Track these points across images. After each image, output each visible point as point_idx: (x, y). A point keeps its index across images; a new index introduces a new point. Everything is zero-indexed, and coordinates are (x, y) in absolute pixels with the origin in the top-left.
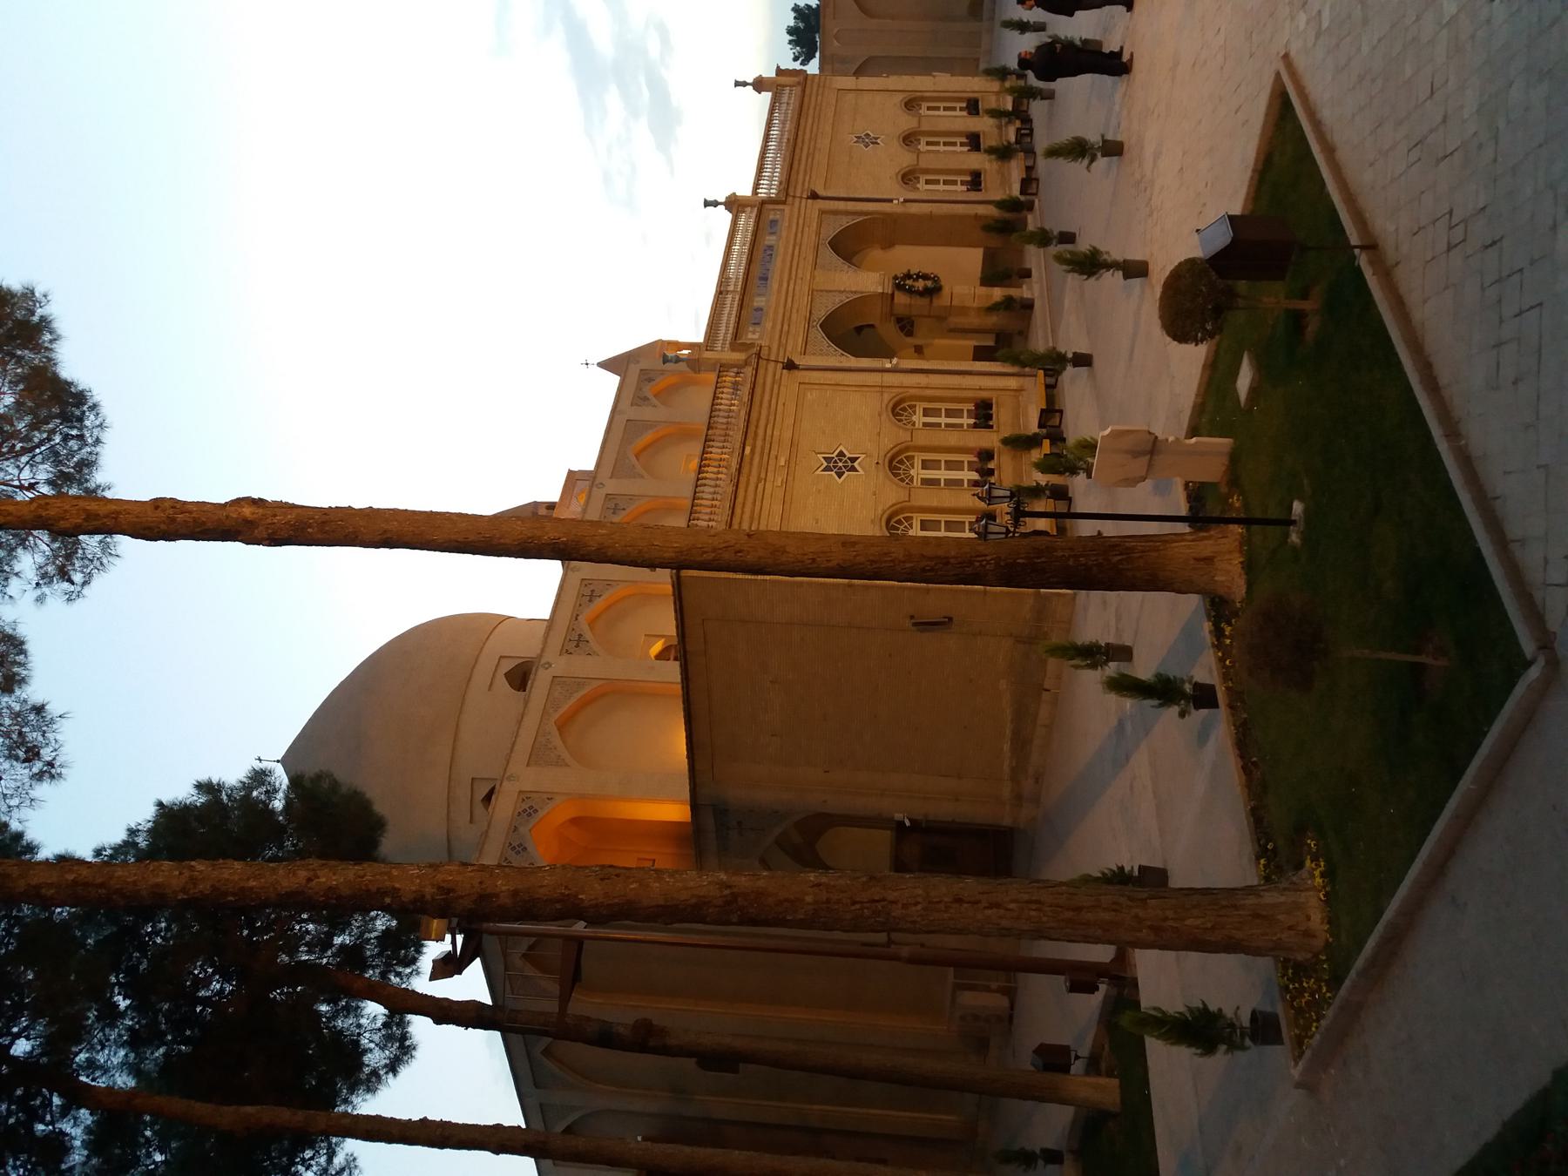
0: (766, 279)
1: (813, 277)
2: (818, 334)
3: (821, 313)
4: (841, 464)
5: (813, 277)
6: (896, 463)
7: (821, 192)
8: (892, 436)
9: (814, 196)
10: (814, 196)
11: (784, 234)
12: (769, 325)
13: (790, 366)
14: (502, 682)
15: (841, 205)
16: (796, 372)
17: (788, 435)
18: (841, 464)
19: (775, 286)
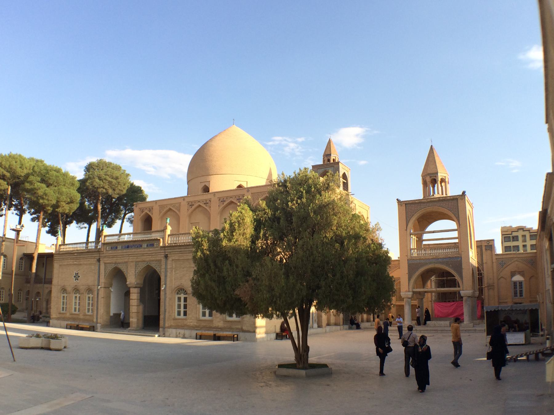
0: (128, 247)
1: (132, 262)
2: (113, 266)
3: (120, 266)
4: (77, 277)
5: (132, 262)
6: (76, 290)
7: (170, 259)
8: (82, 288)
9: (166, 257)
10: (166, 257)
11: (146, 250)
12: (110, 252)
13: (99, 260)
14: (203, 185)
15: (163, 267)
16: (98, 263)
17: (82, 263)
18: (77, 277)
19: (125, 251)
